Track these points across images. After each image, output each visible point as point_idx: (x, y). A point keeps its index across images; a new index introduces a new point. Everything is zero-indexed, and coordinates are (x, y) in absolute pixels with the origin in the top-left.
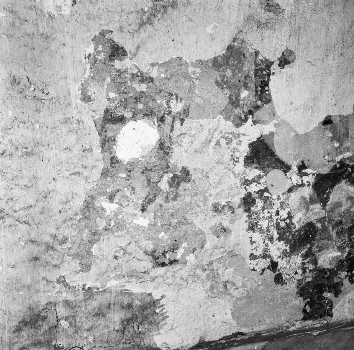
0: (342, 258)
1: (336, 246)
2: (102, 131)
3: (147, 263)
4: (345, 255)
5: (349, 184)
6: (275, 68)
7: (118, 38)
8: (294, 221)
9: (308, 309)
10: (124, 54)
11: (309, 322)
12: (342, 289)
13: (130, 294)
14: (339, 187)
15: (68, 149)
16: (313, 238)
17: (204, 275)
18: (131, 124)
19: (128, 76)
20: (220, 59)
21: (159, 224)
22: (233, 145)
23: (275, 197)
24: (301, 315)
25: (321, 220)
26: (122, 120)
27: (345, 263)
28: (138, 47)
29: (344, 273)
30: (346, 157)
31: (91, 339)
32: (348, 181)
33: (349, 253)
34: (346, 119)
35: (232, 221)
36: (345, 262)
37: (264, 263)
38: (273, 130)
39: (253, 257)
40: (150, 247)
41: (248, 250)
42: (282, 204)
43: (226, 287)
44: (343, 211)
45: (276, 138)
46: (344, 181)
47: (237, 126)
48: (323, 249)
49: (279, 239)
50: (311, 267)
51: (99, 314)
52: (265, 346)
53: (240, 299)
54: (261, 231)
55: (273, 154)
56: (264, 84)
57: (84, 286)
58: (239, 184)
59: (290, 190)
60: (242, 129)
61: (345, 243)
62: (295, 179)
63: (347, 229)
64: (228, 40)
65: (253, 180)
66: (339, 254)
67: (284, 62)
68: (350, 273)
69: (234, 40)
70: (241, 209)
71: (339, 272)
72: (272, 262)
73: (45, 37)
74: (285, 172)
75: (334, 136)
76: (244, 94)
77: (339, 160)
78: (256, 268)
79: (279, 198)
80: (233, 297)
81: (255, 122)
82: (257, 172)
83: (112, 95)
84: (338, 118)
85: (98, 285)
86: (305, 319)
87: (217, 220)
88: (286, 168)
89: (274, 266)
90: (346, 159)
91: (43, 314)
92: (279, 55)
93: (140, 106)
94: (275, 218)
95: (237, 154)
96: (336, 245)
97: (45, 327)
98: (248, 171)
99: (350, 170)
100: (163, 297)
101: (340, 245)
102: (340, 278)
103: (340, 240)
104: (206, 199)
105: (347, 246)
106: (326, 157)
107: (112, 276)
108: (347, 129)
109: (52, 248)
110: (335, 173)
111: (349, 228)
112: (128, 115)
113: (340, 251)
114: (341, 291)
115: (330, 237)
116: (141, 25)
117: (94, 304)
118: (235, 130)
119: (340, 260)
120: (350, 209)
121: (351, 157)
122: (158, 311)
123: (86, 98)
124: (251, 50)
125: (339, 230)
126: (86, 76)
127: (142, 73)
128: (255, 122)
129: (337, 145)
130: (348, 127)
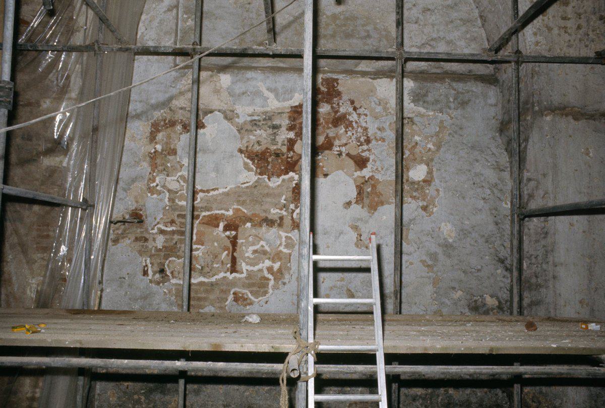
2: (432, 178)
3: (416, 119)
6: (354, 201)
7: (424, 213)
8: (344, 129)
9: (335, 84)
10: (422, 208)
11: (335, 76)
13: (424, 107)
15: (446, 171)
16: (333, 120)
17: (390, 110)
18: (420, 179)
19: (420, 199)
20: (380, 205)
21: (410, 136)
22: (375, 168)
23: (354, 142)
24: (339, 81)
25: (329, 128)
26: (424, 181)
31: (441, 91)
35: (376, 133)
37: (361, 111)
38: (355, 173)
39: (366, 115)
40: (414, 126)
41: (368, 118)
42: (351, 138)
43: (380, 103)
45: (354, 169)
47: (373, 176)
48: (328, 114)
49: (352, 122)
50: (334, 105)
52: (355, 68)
53: (372, 96)
54: (361, 127)
55: (355, 162)
56: (359, 194)
57: (443, 114)
58: (372, 150)
59: (346, 144)
60: (371, 174)
62: (343, 149)
64: (376, 213)
65: (365, 151)
67: (348, 204)
69: (373, 213)
70: (371, 138)
72: (356, 111)
73: (451, 214)
74: (348, 153)
76: (369, 190)
78: (364, 110)
79: (352, 141)
80: (376, 98)
81: (364, 177)
82: (363, 154)
83: (428, 191)
85: (437, 114)
86: (337, 79)
87: (384, 134)
88: (348, 155)
89: (355, 109)
91: (459, 105)
92: (352, 207)
93: (416, 186)
94: (354, 132)
95: (373, 163)
97: (459, 100)
98: (368, 155)
100: (409, 104)
104: (388, 145)
106: (326, 158)
107: (431, 117)
109: (454, 132)
112: (422, 183)
115: (324, 119)
116: (414, 219)
117: (439, 106)
118: (374, 174)
122: (412, 98)
123: (438, 190)
124: (365, 209)
126: (437, 199)
127: (415, 200)
128: (364, 177)
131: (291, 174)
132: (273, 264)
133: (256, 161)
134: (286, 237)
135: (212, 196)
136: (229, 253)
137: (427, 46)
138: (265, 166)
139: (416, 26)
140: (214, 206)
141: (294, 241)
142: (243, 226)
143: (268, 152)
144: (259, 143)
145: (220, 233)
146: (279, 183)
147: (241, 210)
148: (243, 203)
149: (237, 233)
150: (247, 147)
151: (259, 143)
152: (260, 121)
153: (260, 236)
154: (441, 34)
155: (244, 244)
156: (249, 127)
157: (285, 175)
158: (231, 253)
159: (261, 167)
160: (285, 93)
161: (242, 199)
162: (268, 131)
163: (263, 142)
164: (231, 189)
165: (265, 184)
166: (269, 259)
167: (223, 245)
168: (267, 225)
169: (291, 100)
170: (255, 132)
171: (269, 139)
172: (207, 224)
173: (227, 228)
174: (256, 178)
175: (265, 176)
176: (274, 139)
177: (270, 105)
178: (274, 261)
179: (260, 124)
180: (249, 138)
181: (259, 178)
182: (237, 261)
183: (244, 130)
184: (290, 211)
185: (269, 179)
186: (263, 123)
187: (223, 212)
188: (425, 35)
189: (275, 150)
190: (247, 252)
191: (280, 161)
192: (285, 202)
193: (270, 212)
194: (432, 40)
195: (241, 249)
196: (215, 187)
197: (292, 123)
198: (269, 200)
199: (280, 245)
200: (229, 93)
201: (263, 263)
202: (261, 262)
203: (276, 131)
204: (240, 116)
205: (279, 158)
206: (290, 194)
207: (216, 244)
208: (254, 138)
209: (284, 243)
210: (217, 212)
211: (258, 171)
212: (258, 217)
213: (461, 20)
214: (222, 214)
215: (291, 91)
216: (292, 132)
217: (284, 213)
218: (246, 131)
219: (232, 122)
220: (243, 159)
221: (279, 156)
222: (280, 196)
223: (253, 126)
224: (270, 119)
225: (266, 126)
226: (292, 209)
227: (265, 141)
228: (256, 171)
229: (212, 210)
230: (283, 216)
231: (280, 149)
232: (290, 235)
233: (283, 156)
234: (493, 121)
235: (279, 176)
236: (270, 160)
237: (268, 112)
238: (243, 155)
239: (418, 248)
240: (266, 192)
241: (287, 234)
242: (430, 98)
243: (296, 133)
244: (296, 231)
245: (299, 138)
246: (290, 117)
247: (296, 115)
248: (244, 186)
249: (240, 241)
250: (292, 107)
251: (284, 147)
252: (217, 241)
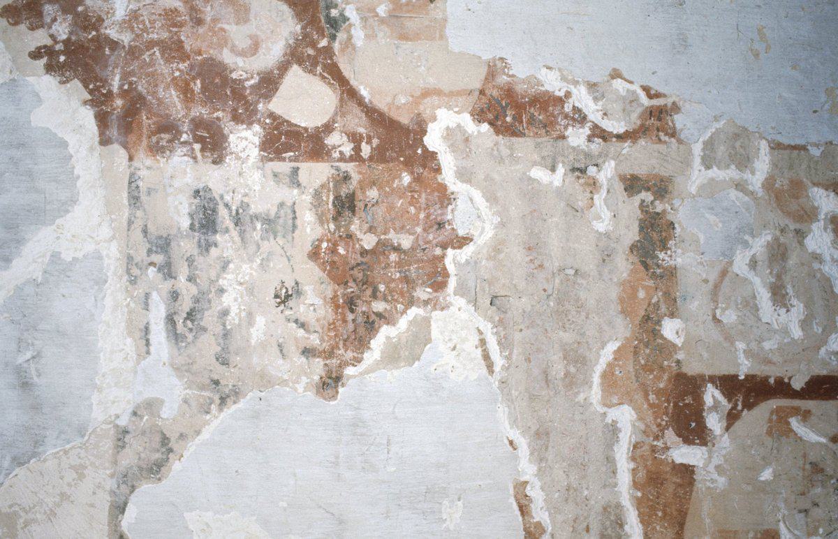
0: (105, 24)
1: (141, 5)
4: (113, 33)
5: (291, 42)
12: (23, 27)
14: (285, 17)
27: (90, 33)
29: (66, 31)
30: (353, 32)
32: (297, 40)
33: (114, 45)
34: (438, 35)
36: (94, 33)
44: (226, 27)
46: (298, 28)
61: (145, 30)
63: (179, 37)
66: (120, 12)
68: (62, 48)
71: (70, 17)
75: (401, 5)
77: (347, 14)
84: (440, 16)
90: (349, 32)
96: (145, 5)
99: (323, 43)
101: (141, 18)
102: (54, 20)
103: (154, 17)
105: (137, 36)
108: (416, 37)
110: (317, 6)
111: (182, 42)
113: (127, 18)
114: (16, 24)
119: (103, 20)
120: (229, 45)
121: (354, 48)
125: (181, 16)
129: (382, 10)
130: (420, 39)
131: (433, 140)
132: (822, 216)
133: (379, 306)
134: (707, 163)
135: (553, 509)
136: (796, 411)
138: (399, 264)
140: (599, 498)
141: (718, 131)
142: (680, 356)
143: (333, 251)
144: (284, 299)
145: (716, 461)
146: (477, 195)
147: (610, 365)
148: (577, 359)
149: (712, 379)
150: (308, 352)
151: (284, 299)
152: (175, 296)
153: (713, 276)
155: (754, 345)
156: (208, 346)
157: (438, 170)
158: (797, 403)
159: (406, 279)
160: (30, 174)
161: (558, 369)
162: (229, 253)
163: (281, 273)
164: (514, 422)
165: (484, 262)
166: (801, 235)
167: (769, 441)
168: (664, 248)
169: (64, 144)
170: (233, 318)
171: (265, 245)
172: (682, 525)
173: (693, 431)
174: (460, 302)
175: (449, 263)
176: (268, 221)
177: (90, 247)
178: (807, 215)
179: (188, 291)
180: (263, 345)
181: (461, 290)
182: (824, 372)
183: (219, 371)
184: (597, 146)
185: (463, 242)
186: (182, 278)
187: (622, 453)
189: (321, 219)
190: (785, 331)
191: (373, 194)
192: (561, 170)
193: (607, 235)
195: (776, 358)
196: (512, 501)
197: (184, 137)
198: (554, 242)
199: (740, 186)
200: (19, 462)
201: (817, 257)
202: (816, 266)
203: (224, 216)
204: (149, 394)
205: (359, 195)
206: (525, 146)
207: (767, 475)
208: (260, 321)
209: (732, 173)
210: (624, 478)
211: (423, 293)
212: (634, 291)
214: (633, 459)
215: (21, 145)
216: (232, 138)
217: (606, 173)
218: (225, 363)
219: (182, 436)
220: (368, 371)
221: (352, 197)
222: (532, 192)
223: (204, 330)
224: (163, 244)
225: (200, 260)
226: (590, 139)
227: (279, 263)
228: (426, 303)
229: (619, 506)
230: (623, 178)
231: (317, 195)
232: (697, 149)
233: (347, 178)
235: (444, 197)
236: (369, 242)
237: (130, 258)
238: (349, 371)
240: (516, 254)
241: (697, 161)
243: (236, 119)
244: (679, 120)
245: (260, 106)
246: (156, 150)
247: (145, 120)
248: (499, 362)
249: (744, 367)
250: (105, 141)
251: (302, 176)
252: (756, 469)
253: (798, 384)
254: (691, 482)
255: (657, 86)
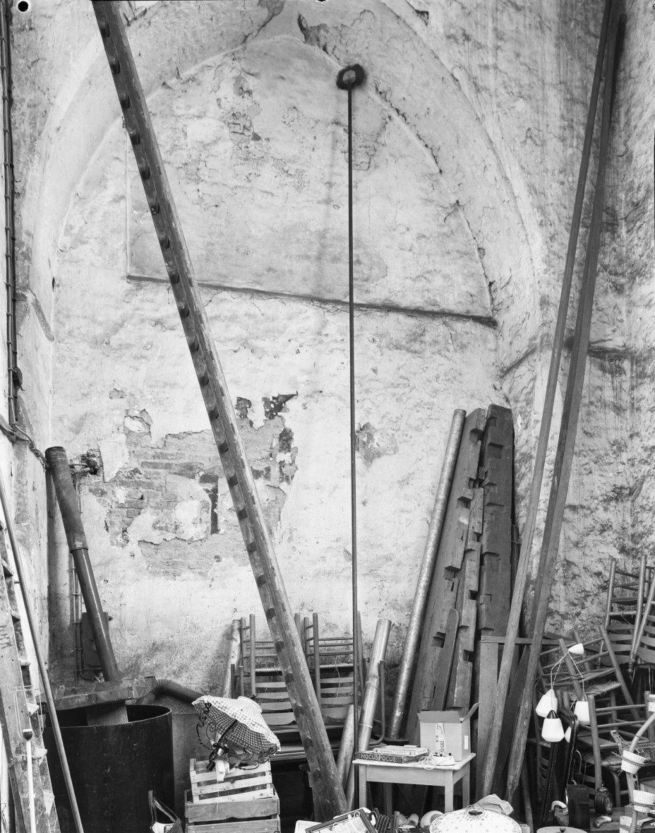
28: (415, 463)
51: (436, 342)
76: (365, 439)
117: (437, 347)
137: (423, 279)
139: (411, 254)
149: (217, 486)
154: (437, 267)
159: (242, 409)
188: (420, 266)
194: (428, 272)
213: (458, 251)
234: (493, 368)
239: (419, 505)
242: (427, 338)
253: (215, 510)
254: (190, 478)
255: (295, 479)
